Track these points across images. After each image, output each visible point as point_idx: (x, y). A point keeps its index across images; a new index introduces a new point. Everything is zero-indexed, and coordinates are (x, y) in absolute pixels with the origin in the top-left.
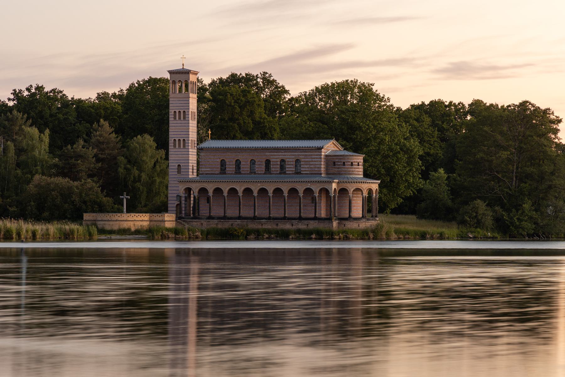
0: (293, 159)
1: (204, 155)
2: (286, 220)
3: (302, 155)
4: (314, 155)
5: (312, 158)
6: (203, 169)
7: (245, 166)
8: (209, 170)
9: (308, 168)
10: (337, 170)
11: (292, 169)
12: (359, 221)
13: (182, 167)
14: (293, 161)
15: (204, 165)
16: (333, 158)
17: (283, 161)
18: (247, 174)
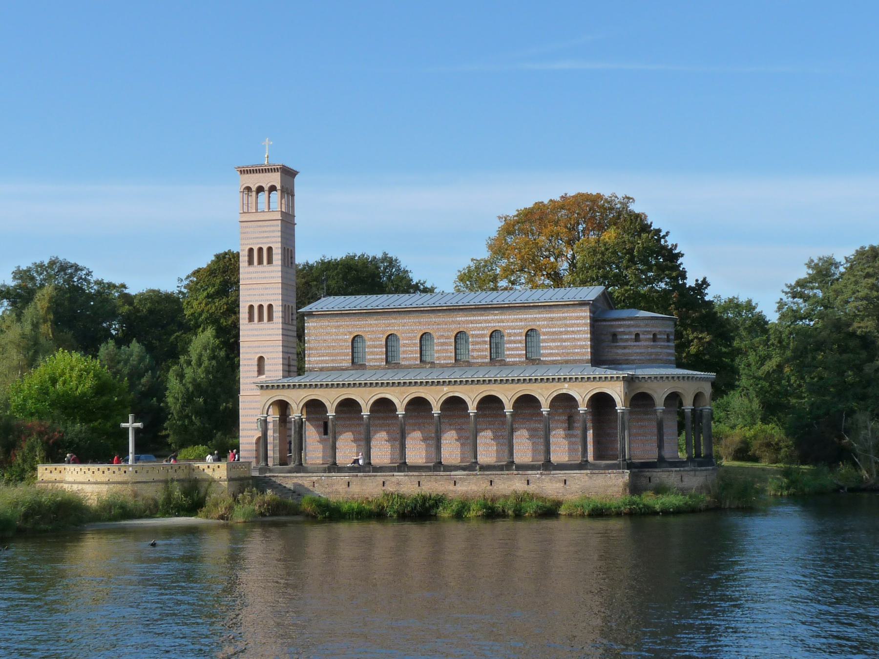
0: (522, 328)
1: (314, 327)
2: (513, 470)
3: (542, 318)
4: (571, 318)
5: (566, 326)
6: (312, 359)
7: (410, 349)
8: (326, 360)
9: (557, 347)
10: (620, 351)
11: (520, 352)
12: (682, 469)
13: (266, 362)
14: (520, 334)
15: (316, 349)
16: (612, 326)
17: (495, 334)
18: (415, 367)
